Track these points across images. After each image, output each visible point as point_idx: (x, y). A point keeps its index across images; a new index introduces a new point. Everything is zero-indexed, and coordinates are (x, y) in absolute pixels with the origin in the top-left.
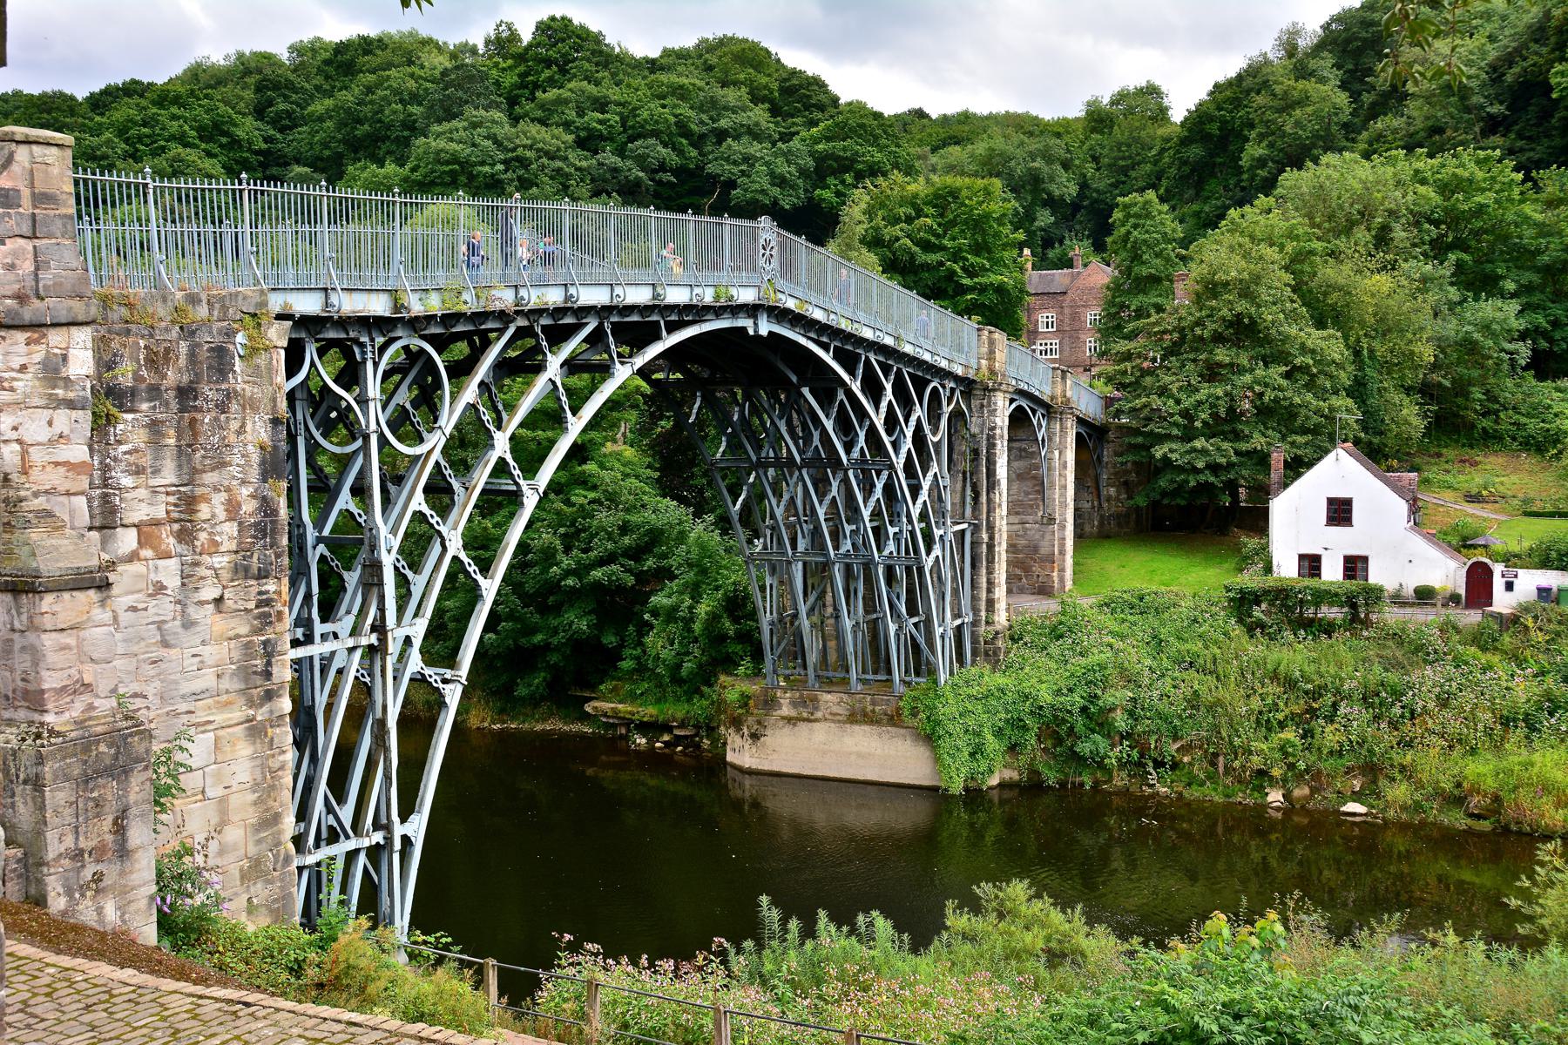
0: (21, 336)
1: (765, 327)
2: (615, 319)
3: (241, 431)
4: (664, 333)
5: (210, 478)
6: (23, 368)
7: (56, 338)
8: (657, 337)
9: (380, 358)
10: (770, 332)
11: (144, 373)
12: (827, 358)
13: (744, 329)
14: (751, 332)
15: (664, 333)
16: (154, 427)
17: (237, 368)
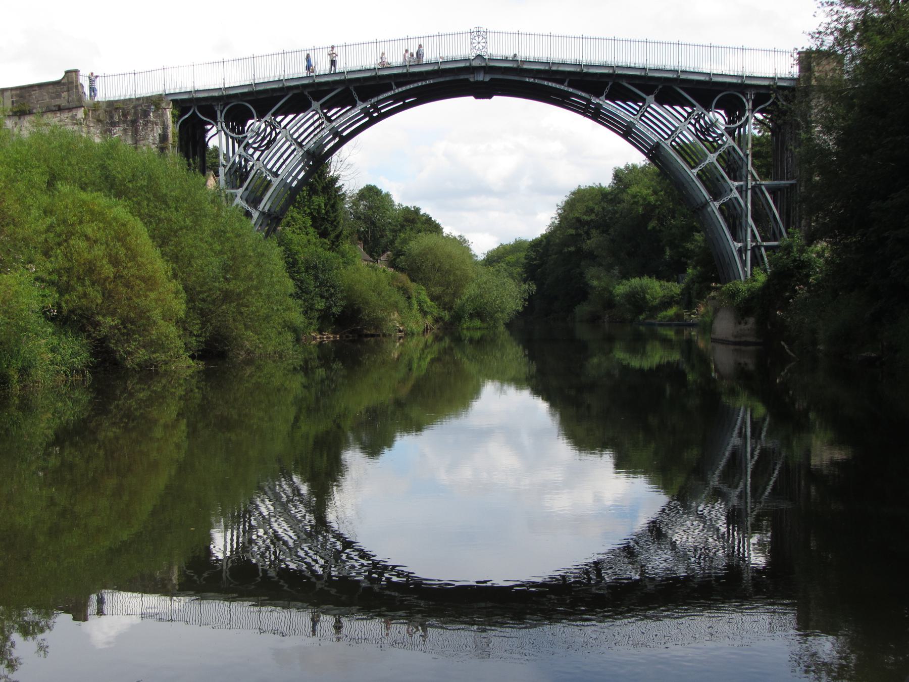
0: (67, 111)
1: (481, 77)
2: (358, 85)
3: (152, 130)
4: (394, 87)
5: (142, 142)
6: (67, 118)
7: (74, 112)
8: (391, 89)
9: (224, 108)
10: (491, 80)
11: (121, 118)
12: (562, 87)
13: (467, 80)
14: (472, 80)
15: (394, 87)
16: (125, 130)
17: (151, 114)
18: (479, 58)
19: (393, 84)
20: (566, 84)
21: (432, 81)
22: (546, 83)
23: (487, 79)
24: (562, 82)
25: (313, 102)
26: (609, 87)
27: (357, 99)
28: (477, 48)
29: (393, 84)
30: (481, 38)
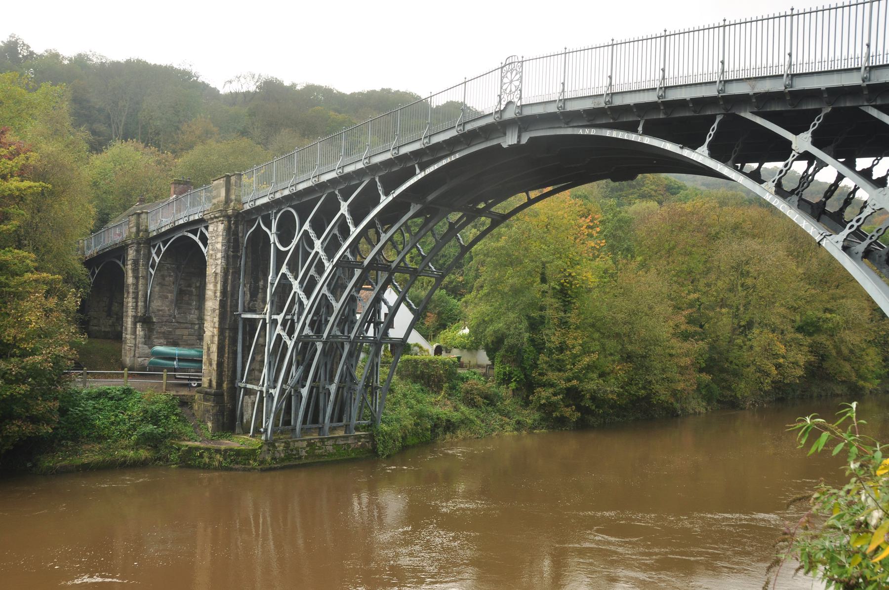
1: (510, 140)
4: (418, 171)
8: (414, 174)
10: (531, 139)
12: (633, 137)
14: (505, 146)
18: (523, 108)
19: (416, 166)
20: (640, 129)
21: (457, 156)
22: (608, 133)
23: (524, 140)
24: (635, 131)
25: (342, 203)
26: (715, 125)
27: (381, 193)
28: (508, 91)
29: (416, 166)
30: (514, 72)
